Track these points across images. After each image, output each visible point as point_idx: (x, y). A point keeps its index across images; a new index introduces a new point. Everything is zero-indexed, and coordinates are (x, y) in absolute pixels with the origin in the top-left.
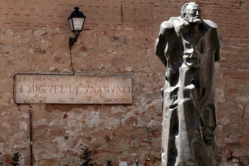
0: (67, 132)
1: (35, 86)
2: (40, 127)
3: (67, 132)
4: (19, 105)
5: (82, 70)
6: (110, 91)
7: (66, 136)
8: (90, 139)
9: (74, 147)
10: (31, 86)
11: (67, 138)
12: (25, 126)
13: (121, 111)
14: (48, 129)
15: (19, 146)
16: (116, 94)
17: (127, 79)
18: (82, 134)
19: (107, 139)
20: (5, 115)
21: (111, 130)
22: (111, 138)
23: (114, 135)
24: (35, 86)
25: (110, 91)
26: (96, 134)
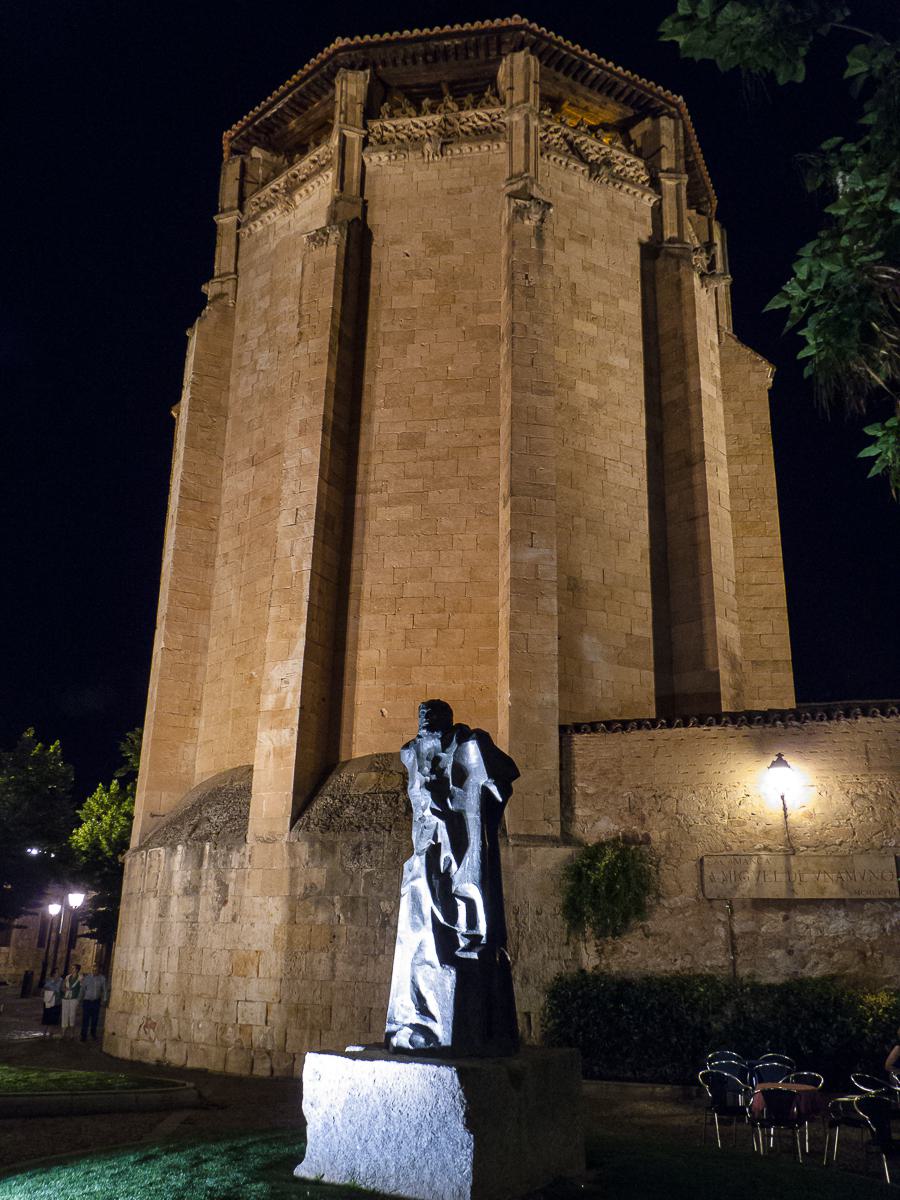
0: (791, 943)
1: (732, 873)
2: (744, 934)
3: (791, 943)
4: (710, 900)
5: (808, 847)
6: (858, 878)
7: (789, 948)
8: (831, 955)
9: (803, 968)
10: (726, 872)
11: (790, 952)
12: (721, 932)
13: (882, 909)
14: (760, 939)
15: (714, 962)
16: (869, 883)
17: (886, 859)
18: (817, 947)
19: (862, 954)
20: (690, 916)
21: (868, 941)
22: (869, 954)
23: (873, 950)
24: (732, 873)
25: (858, 878)
26: (841, 947)
